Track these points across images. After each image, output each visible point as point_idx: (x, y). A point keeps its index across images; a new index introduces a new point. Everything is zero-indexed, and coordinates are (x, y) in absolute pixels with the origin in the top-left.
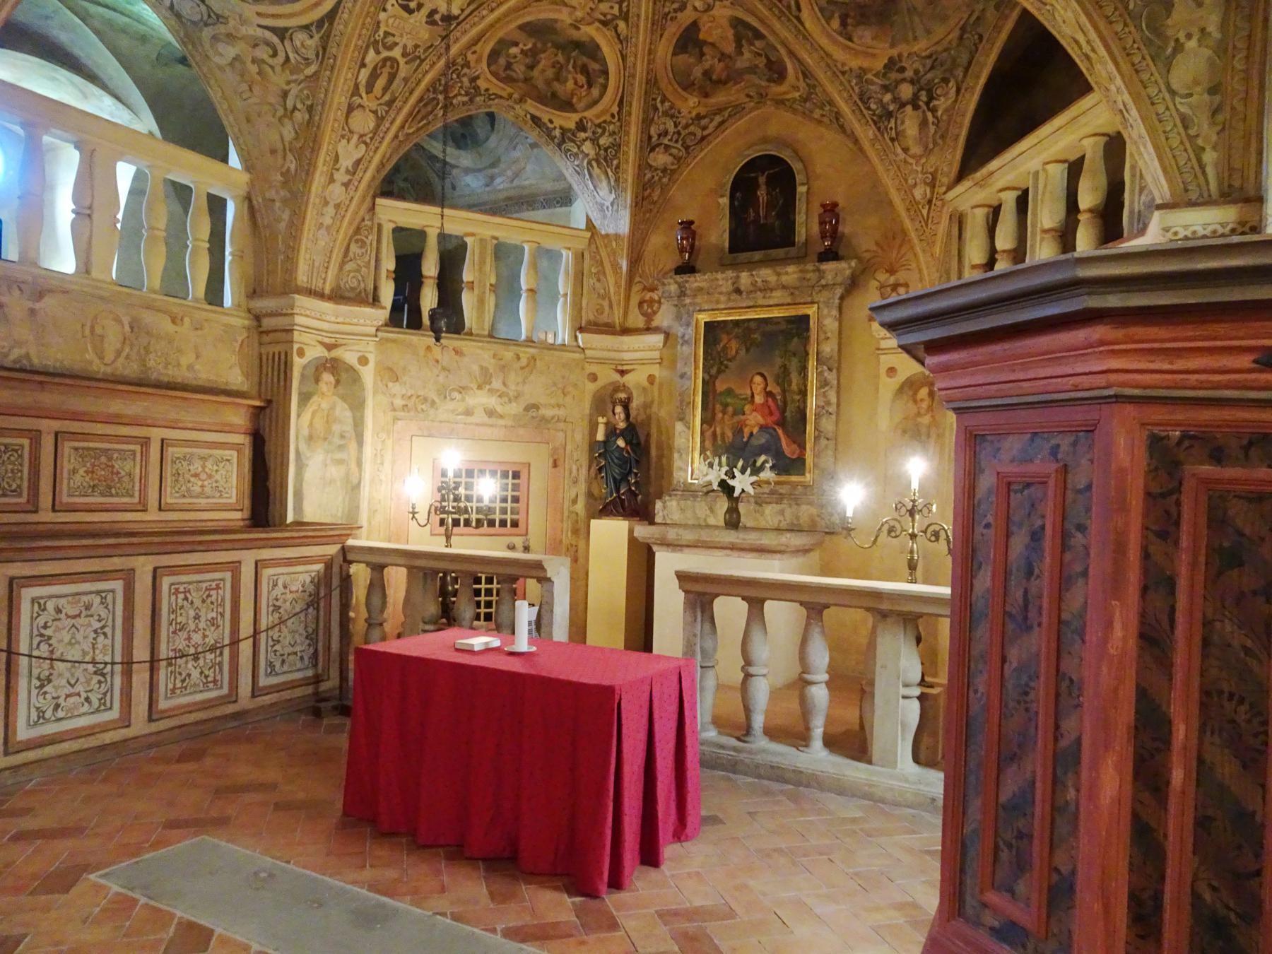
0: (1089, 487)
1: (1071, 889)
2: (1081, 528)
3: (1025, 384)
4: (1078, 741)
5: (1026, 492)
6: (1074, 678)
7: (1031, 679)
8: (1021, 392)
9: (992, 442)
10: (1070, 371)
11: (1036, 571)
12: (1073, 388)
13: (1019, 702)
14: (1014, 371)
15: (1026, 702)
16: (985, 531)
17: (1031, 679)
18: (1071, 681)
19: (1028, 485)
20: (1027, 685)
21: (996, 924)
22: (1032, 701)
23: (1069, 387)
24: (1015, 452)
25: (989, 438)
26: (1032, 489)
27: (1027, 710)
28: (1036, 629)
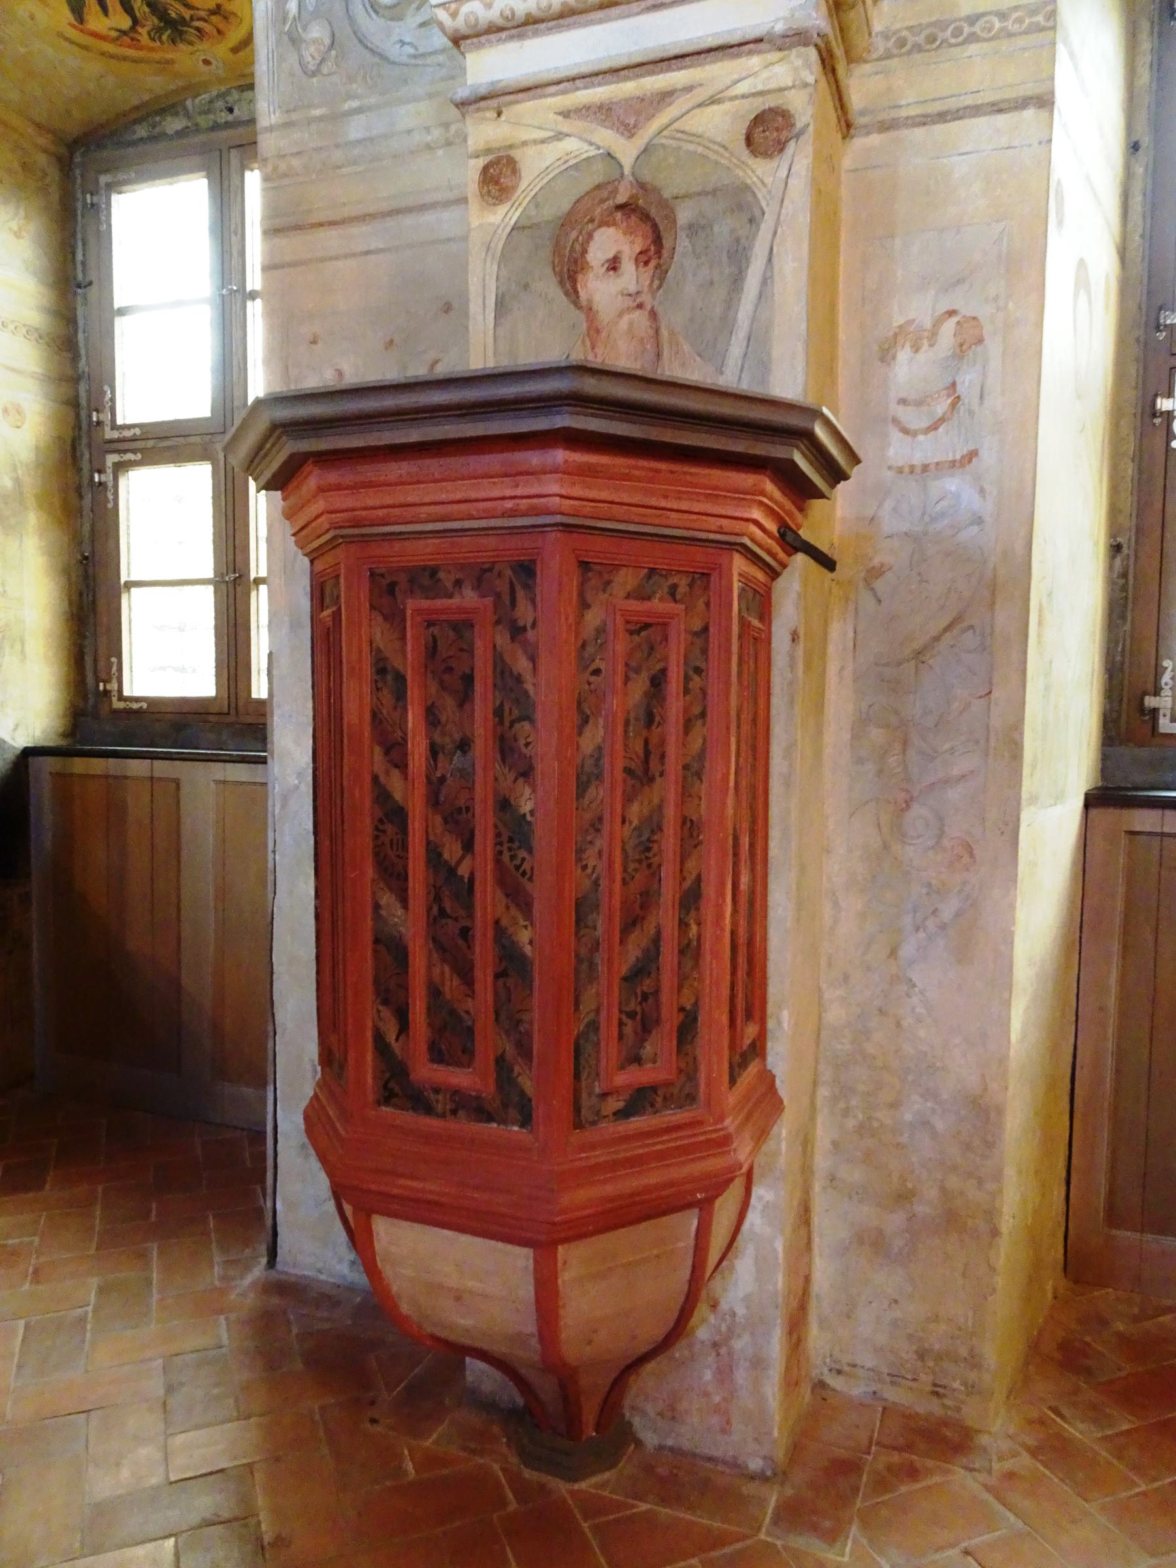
0: (706, 629)
1: (695, 1019)
2: (698, 671)
3: (673, 515)
4: (699, 879)
5: (643, 634)
6: (694, 818)
7: (653, 832)
8: (665, 522)
9: (600, 573)
10: (723, 512)
11: (657, 719)
12: (718, 530)
13: (640, 861)
14: (680, 498)
15: (647, 858)
16: (593, 679)
17: (653, 832)
18: (691, 821)
19: (647, 626)
20: (649, 840)
21: (621, 1104)
22: (655, 855)
23: (713, 528)
24: (629, 588)
25: (598, 568)
26: (651, 630)
27: (649, 866)
28: (658, 780)
